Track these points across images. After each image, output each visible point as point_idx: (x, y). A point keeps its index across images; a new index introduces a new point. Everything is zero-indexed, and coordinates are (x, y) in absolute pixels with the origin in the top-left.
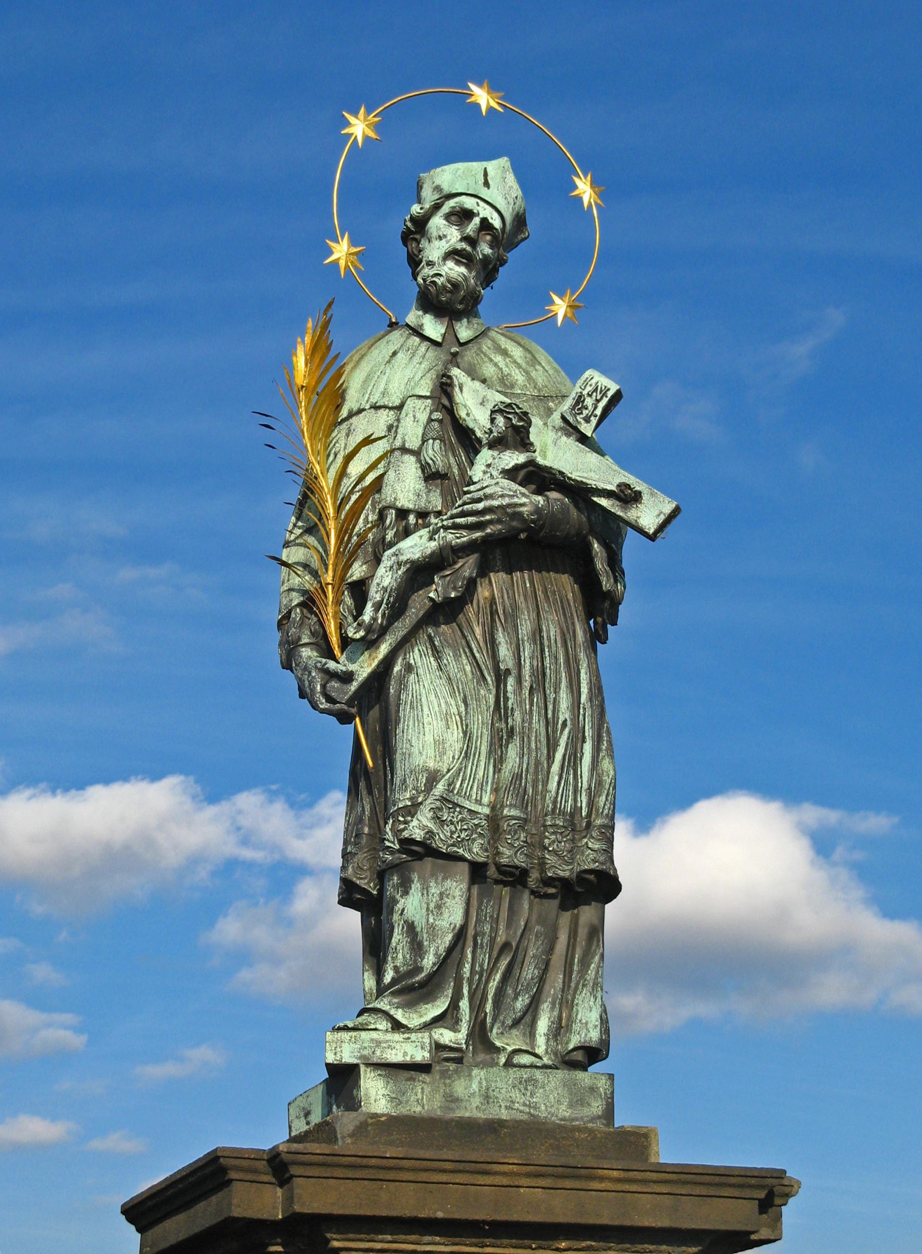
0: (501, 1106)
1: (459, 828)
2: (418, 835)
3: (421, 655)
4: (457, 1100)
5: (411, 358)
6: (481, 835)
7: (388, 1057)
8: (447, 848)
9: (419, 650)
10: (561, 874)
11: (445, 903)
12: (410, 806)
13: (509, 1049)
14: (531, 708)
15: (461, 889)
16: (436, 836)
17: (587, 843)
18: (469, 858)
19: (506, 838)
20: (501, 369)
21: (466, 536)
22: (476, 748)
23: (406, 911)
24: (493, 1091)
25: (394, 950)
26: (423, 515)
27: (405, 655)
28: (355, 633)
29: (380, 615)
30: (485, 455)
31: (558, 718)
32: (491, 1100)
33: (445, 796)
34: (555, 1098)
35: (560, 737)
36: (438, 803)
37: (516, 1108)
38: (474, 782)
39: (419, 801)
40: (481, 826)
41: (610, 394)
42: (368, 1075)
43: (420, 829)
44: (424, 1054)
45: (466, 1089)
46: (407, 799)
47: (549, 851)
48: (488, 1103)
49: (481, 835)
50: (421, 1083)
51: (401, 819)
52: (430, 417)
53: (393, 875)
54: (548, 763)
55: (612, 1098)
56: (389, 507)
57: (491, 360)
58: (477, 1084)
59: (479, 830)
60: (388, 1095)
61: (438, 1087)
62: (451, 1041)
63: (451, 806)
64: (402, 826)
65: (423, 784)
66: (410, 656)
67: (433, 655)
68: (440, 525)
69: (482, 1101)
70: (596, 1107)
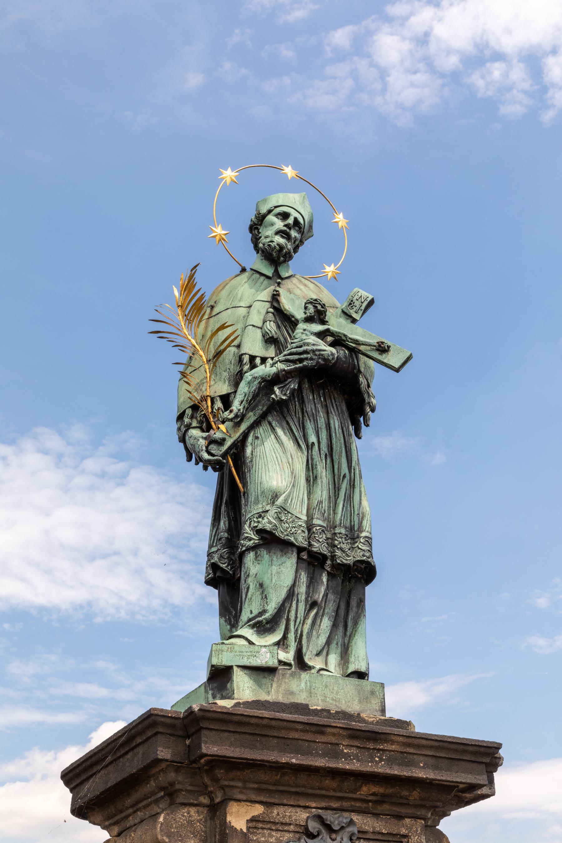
0: (318, 699)
1: (291, 525)
2: (268, 527)
3: (264, 431)
4: (292, 693)
5: (255, 284)
6: (303, 531)
7: (252, 662)
8: (284, 537)
9: (263, 429)
10: (345, 561)
11: (282, 571)
12: (261, 512)
13: (318, 667)
14: (326, 466)
15: (292, 563)
16: (278, 528)
17: (358, 546)
18: (297, 544)
19: (315, 537)
20: (304, 292)
21: (292, 366)
22: (298, 482)
23: (258, 575)
24: (314, 689)
25: (250, 600)
26: (264, 360)
27: (255, 431)
28: (229, 415)
29: (241, 407)
30: (301, 326)
31: (341, 473)
32: (313, 695)
33: (283, 506)
34: (350, 696)
35: (342, 483)
36: (279, 510)
37: (328, 701)
38: (297, 501)
39: (267, 509)
40: (302, 527)
41: (369, 299)
42: (238, 673)
43: (269, 524)
44: (274, 661)
45: (297, 686)
46: (260, 508)
47: (338, 548)
48: (311, 697)
49: (303, 531)
50: (271, 681)
51: (255, 520)
52: (267, 311)
53: (250, 553)
54: (335, 498)
55: (384, 699)
56: (245, 354)
57: (298, 288)
58: (304, 684)
59: (302, 528)
60: (251, 687)
61: (281, 684)
62: (285, 658)
63: (286, 513)
64: (256, 524)
65: (269, 500)
66: (257, 432)
67: (272, 431)
68: (277, 360)
69: (307, 695)
70: (375, 704)
